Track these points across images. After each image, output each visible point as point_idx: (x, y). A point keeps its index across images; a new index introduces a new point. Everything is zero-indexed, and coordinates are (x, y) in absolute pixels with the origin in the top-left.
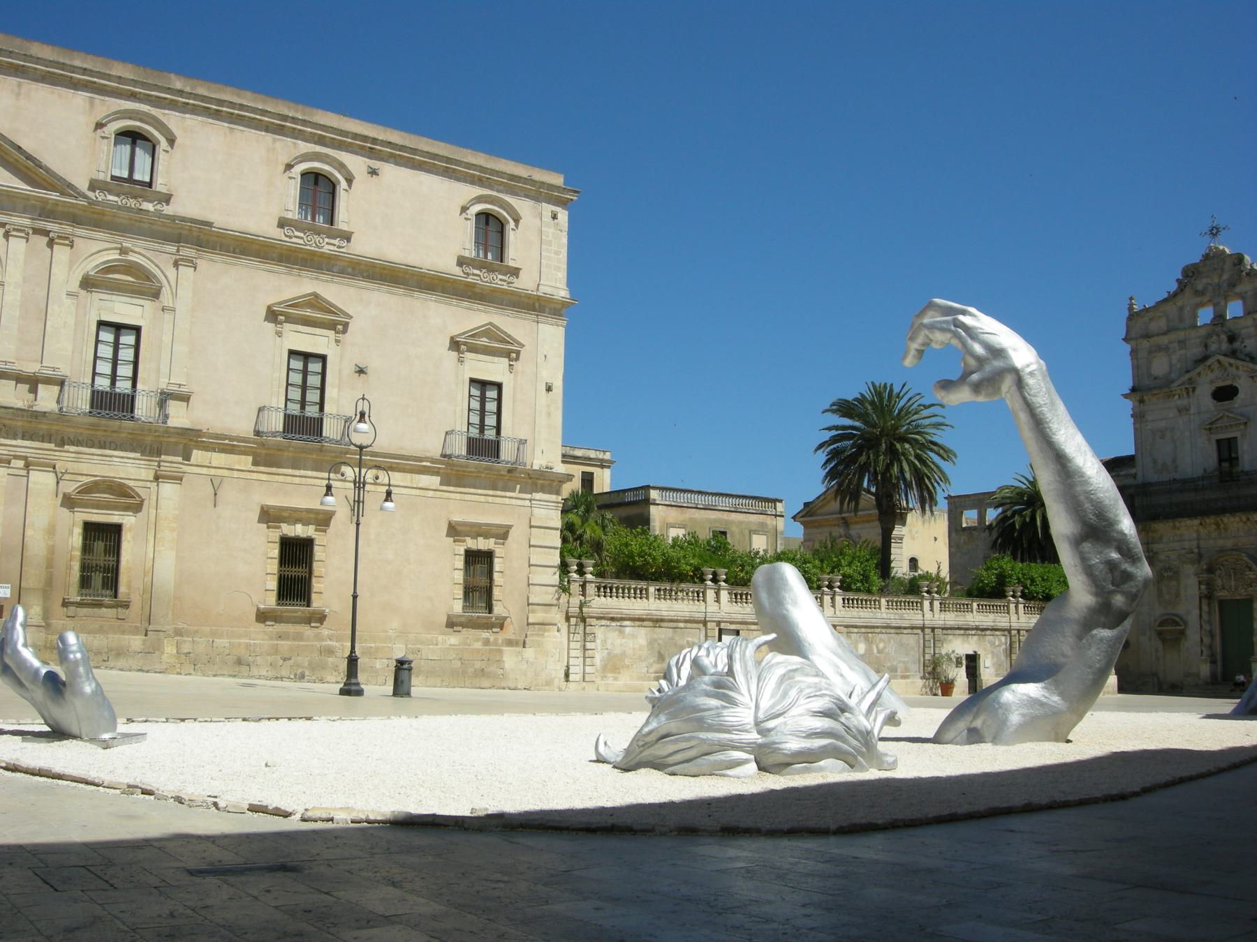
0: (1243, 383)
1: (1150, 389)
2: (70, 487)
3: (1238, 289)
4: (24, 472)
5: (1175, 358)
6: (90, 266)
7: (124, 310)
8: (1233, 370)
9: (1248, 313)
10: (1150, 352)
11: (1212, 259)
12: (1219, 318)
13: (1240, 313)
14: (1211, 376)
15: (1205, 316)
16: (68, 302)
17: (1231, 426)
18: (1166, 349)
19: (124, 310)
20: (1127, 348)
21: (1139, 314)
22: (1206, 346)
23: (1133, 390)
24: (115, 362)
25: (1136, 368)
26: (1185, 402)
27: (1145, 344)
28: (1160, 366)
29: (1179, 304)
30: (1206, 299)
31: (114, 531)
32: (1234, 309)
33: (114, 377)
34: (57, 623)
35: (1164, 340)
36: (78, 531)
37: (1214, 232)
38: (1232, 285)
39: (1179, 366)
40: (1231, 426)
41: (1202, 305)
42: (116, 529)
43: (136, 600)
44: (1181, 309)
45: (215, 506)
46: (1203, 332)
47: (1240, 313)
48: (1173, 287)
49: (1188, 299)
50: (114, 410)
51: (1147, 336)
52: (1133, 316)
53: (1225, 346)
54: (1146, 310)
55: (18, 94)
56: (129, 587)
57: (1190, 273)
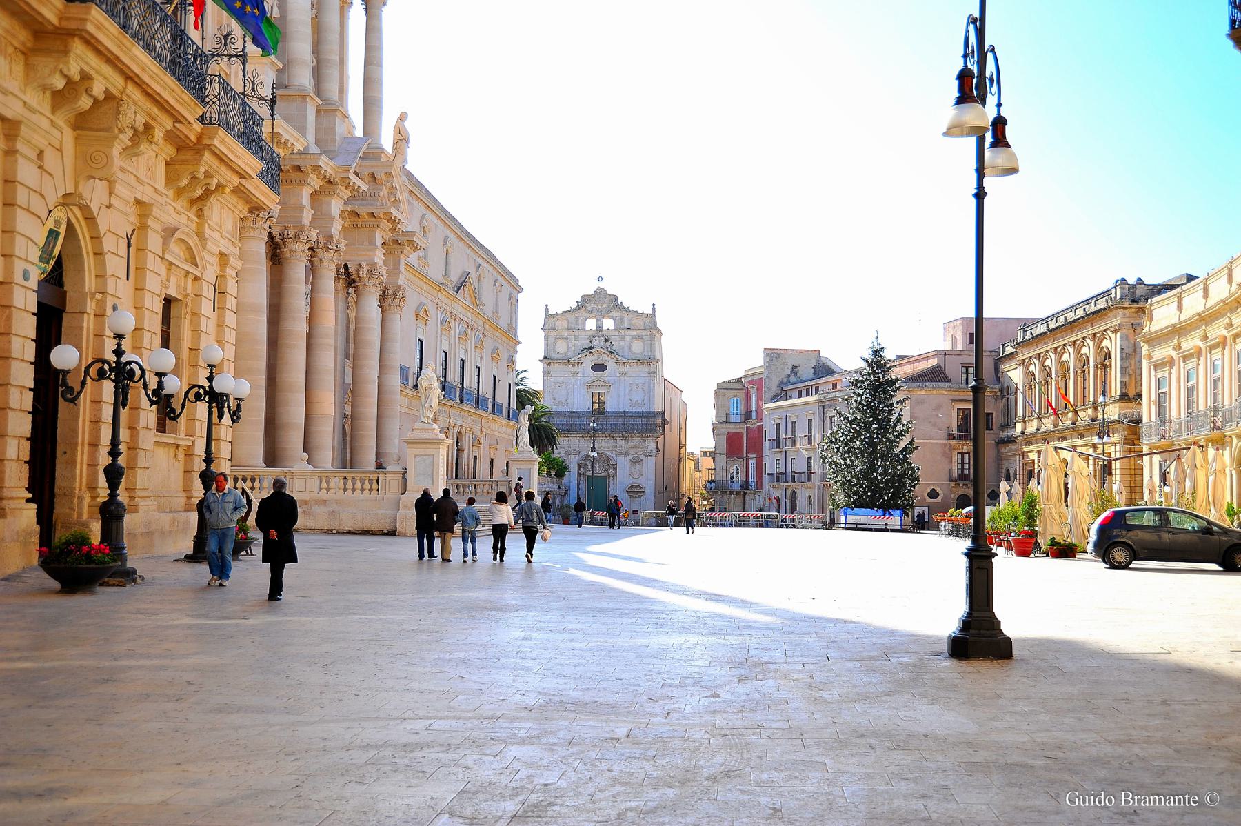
0: (610, 364)
1: (554, 359)
3: (611, 314)
5: (571, 345)
8: (605, 357)
9: (617, 328)
10: (556, 338)
11: (600, 293)
12: (599, 328)
13: (612, 327)
14: (592, 357)
15: (591, 324)
17: (602, 386)
18: (567, 338)
20: (542, 334)
21: (552, 316)
22: (591, 342)
23: (545, 358)
25: (546, 345)
26: (575, 369)
27: (553, 333)
28: (561, 347)
29: (577, 315)
30: (592, 315)
32: (608, 324)
35: (566, 334)
37: (600, 279)
38: (609, 312)
39: (573, 348)
40: (602, 386)
41: (589, 318)
44: (578, 318)
46: (590, 333)
47: (612, 327)
48: (575, 305)
49: (582, 314)
51: (555, 329)
52: (548, 316)
53: (602, 343)
54: (557, 314)
57: (585, 299)
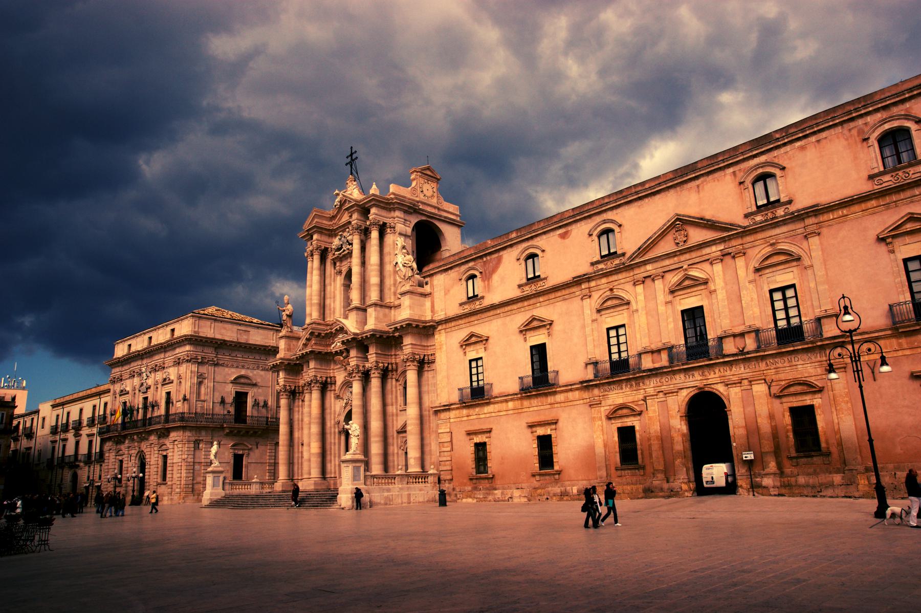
2: (775, 389)
4: (749, 387)
6: (755, 264)
7: (783, 278)
16: (751, 286)
19: (783, 278)
24: (786, 309)
31: (810, 409)
33: (788, 318)
34: (788, 470)
36: (787, 414)
42: (810, 409)
43: (834, 450)
45: (875, 380)
50: (786, 339)
55: (699, 192)
56: (827, 442)
